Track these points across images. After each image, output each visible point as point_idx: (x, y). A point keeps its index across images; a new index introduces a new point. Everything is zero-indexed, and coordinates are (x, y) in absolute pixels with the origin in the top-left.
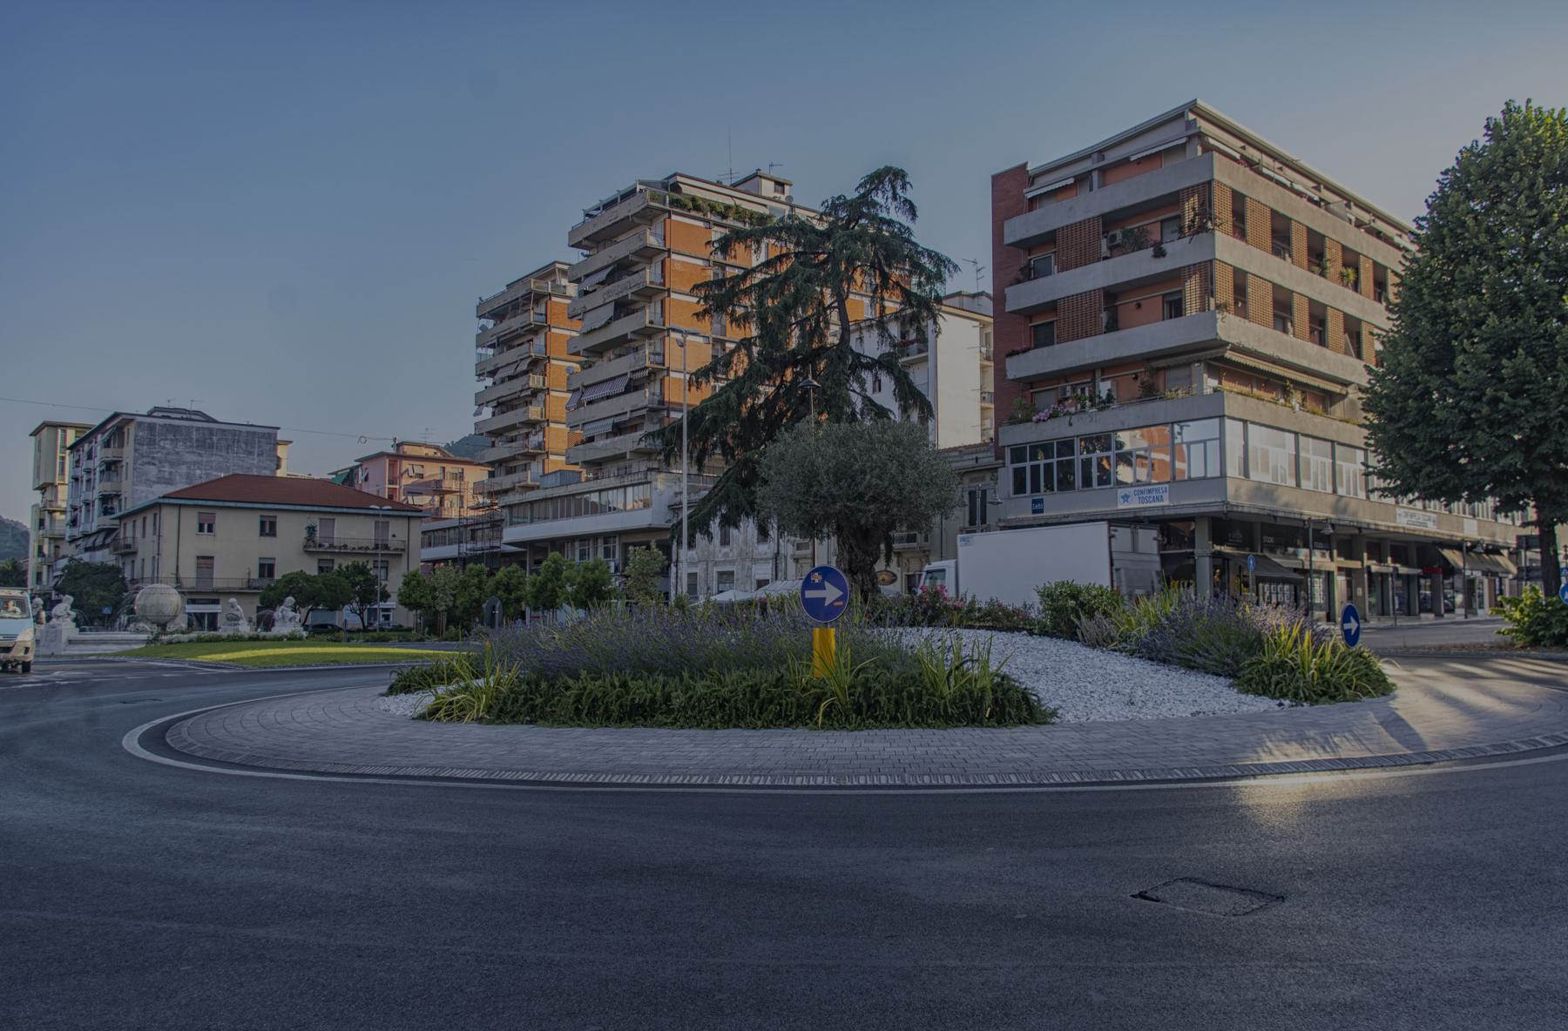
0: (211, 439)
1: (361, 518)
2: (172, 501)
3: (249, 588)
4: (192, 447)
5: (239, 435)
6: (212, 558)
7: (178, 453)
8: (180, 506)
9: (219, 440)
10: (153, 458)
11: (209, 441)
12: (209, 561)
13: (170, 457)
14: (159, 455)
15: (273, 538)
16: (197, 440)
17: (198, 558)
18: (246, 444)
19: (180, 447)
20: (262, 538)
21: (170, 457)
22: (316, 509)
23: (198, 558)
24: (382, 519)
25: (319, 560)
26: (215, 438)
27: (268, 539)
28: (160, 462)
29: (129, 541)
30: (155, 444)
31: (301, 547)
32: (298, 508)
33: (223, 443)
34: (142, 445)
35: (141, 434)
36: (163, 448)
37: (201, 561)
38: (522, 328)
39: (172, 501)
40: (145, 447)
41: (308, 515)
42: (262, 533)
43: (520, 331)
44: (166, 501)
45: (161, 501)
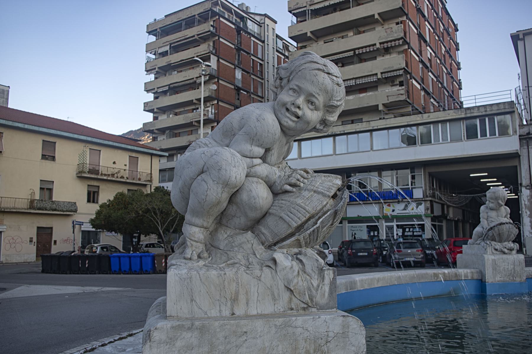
1: (120, 152)
15: (52, 162)
20: (43, 161)
22: (89, 139)
24: (134, 155)
27: (48, 163)
31: (75, 173)
32: (76, 136)
38: (198, 35)
41: (83, 144)
42: (44, 157)
43: (196, 37)
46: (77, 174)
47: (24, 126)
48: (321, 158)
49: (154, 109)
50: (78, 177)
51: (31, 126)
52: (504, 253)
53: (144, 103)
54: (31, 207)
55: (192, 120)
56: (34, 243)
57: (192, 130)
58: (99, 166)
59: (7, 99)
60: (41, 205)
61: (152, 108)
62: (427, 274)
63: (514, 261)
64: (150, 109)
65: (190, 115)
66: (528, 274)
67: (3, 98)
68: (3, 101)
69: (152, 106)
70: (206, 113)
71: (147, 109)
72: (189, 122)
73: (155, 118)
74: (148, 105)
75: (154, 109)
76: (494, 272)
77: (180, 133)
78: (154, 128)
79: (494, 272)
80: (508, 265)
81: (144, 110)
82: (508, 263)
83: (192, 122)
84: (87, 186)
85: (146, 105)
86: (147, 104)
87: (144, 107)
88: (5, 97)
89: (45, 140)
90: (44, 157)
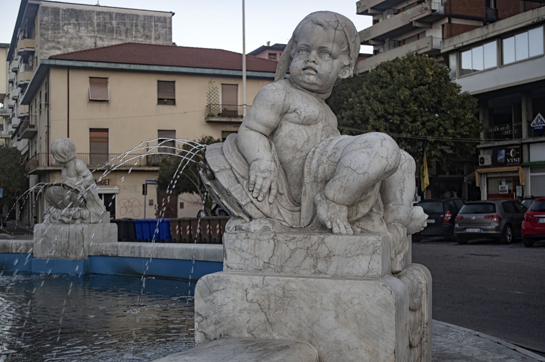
0: (111, 24)
2: (58, 62)
3: (148, 164)
4: (94, 31)
5: (137, 20)
6: (107, 130)
7: (81, 38)
8: (68, 68)
9: (118, 24)
10: (58, 42)
11: (109, 25)
12: (104, 134)
13: (74, 42)
14: (63, 39)
15: (172, 107)
16: (98, 25)
17: (91, 130)
18: (144, 27)
19: (83, 32)
21: (74, 42)
22: (217, 72)
23: (91, 130)
25: (223, 132)
26: (114, 23)
27: (166, 109)
28: (65, 47)
29: (33, 124)
30: (58, 29)
31: (203, 117)
32: (198, 71)
33: (123, 28)
34: (47, 29)
35: (45, 18)
36: (67, 32)
37: (95, 134)
39: (58, 62)
40: (50, 32)
42: (161, 101)
44: (52, 62)
45: (47, 62)
46: (206, 118)
47: (130, 66)
48: (527, 63)
49: (367, 10)
50: (209, 122)
51: (138, 66)
52: (63, 222)
53: (357, 3)
54: (148, 164)
55: (411, 20)
56: (155, 206)
57: (418, 35)
58: (237, 105)
59: (170, 28)
60: (155, 161)
61: (366, 9)
62: (173, 249)
63: (69, 233)
64: (364, 10)
65: (409, 12)
66: (96, 250)
67: (166, 27)
68: (166, 31)
69: (365, 6)
70: (428, 7)
71: (360, 12)
72: (408, 22)
73: (375, 22)
74: (361, 5)
75: (367, 10)
76: (44, 245)
77: (404, 40)
78: (369, 39)
79: (44, 245)
80: (61, 238)
81: (358, 14)
82: (62, 235)
83: (411, 23)
84: (220, 133)
85: (359, 6)
86: (360, 4)
87: (358, 8)
88: (168, 26)
89: (161, 80)
90: (161, 101)
